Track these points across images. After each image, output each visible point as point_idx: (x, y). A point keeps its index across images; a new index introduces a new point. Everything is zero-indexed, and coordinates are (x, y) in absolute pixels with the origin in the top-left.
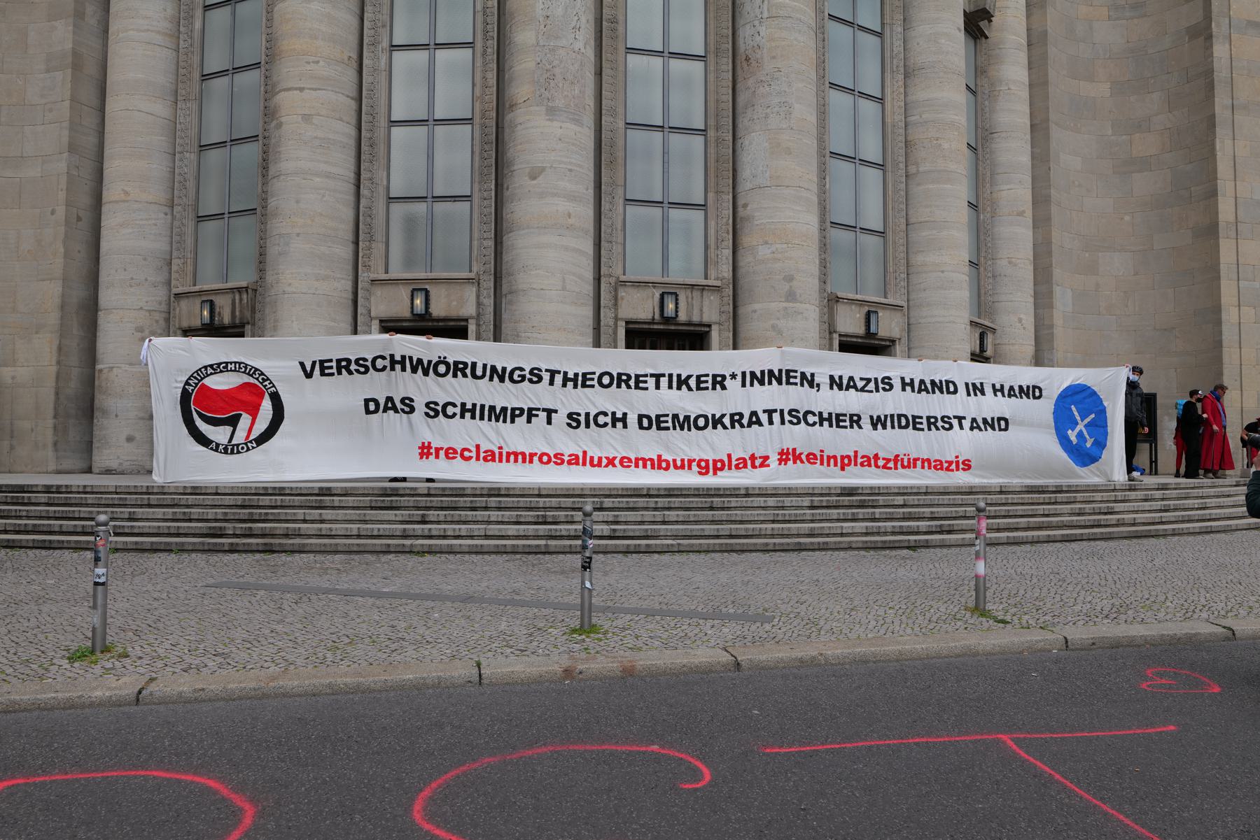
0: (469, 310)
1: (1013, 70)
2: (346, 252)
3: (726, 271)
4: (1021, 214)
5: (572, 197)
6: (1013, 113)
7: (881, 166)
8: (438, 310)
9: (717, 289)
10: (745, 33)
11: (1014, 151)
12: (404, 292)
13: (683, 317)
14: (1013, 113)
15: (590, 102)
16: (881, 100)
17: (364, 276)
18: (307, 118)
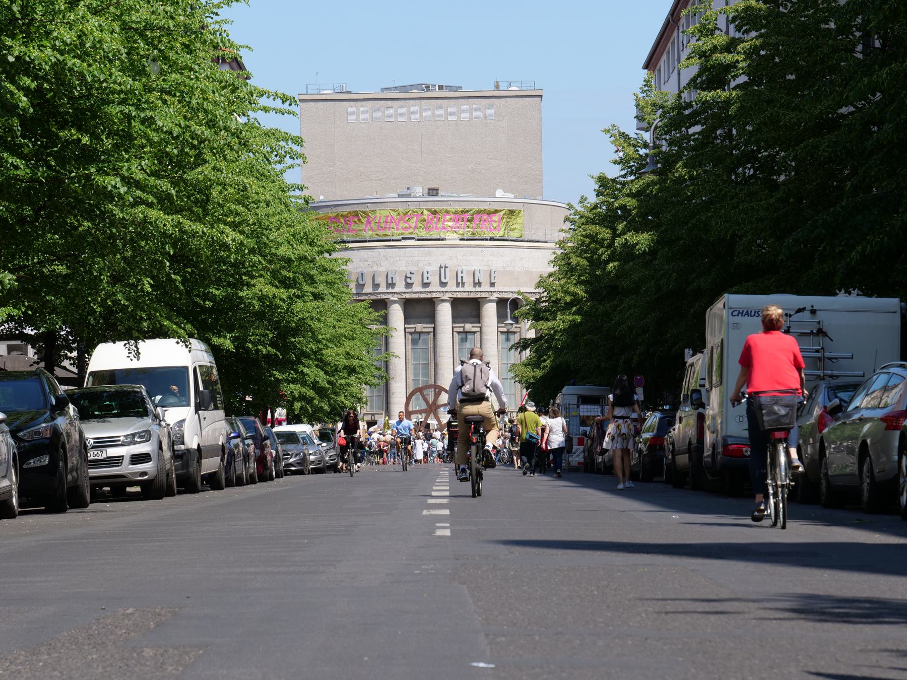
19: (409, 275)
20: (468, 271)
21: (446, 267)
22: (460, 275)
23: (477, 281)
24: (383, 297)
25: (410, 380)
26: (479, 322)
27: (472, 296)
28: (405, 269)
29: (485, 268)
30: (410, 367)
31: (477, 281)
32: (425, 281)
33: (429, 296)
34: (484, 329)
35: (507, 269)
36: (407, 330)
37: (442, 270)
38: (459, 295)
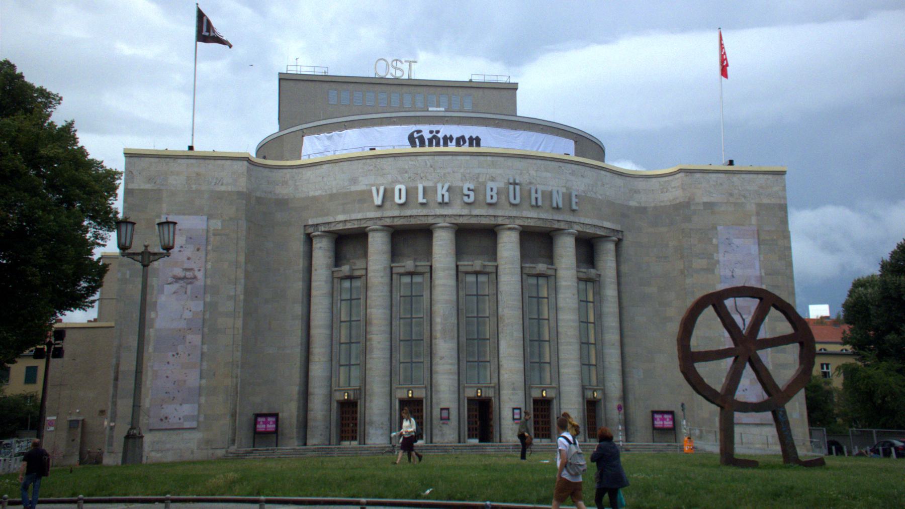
0: (424, 395)
1: (610, 292)
2: (388, 379)
3: (496, 381)
4: (613, 345)
5: (451, 364)
6: (610, 307)
7: (549, 341)
8: (415, 396)
9: (494, 387)
10: (500, 310)
11: (611, 322)
12: (405, 391)
13: (483, 395)
14: (610, 307)
15: (456, 336)
16: (548, 319)
17: (394, 386)
18: (379, 342)
19: (466, 192)
20: (543, 192)
21: (515, 184)
22: (533, 195)
23: (555, 205)
24: (431, 221)
25: (463, 339)
26: (552, 263)
27: (548, 225)
28: (460, 184)
29: (564, 190)
30: (463, 320)
31: (555, 205)
32: (489, 200)
33: (492, 221)
34: (562, 273)
35: (589, 195)
36: (461, 268)
37: (511, 187)
38: (532, 223)
